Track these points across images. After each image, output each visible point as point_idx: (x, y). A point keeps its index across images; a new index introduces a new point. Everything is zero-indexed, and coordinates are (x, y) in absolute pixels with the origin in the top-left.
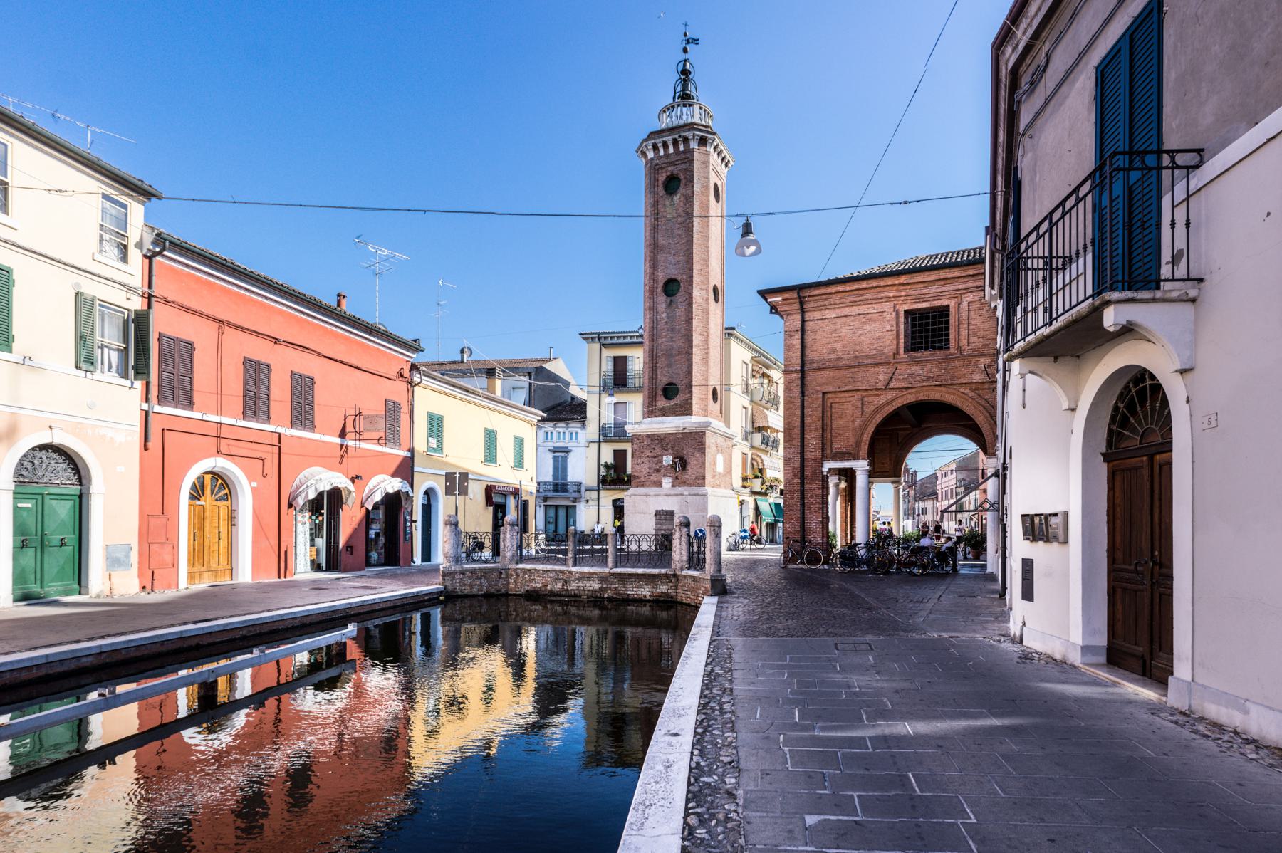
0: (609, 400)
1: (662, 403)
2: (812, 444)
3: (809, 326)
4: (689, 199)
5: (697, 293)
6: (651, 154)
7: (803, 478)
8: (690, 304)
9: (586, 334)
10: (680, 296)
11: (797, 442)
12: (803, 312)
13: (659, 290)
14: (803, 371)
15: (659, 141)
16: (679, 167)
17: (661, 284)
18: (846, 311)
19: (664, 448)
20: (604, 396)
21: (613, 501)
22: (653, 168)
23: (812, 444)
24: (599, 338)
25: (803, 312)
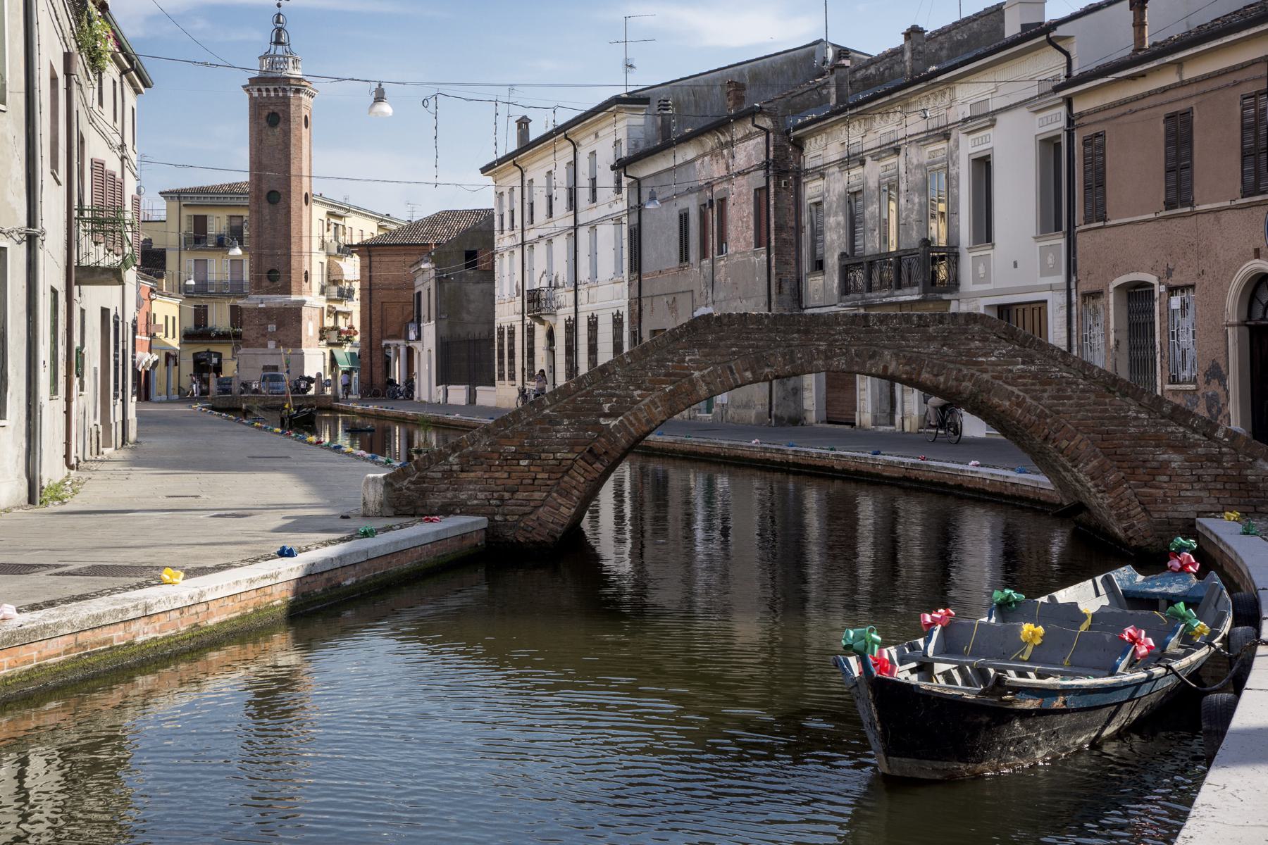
0: (188, 260)
1: (266, 283)
2: (376, 330)
3: (374, 264)
4: (287, 133)
5: (294, 205)
6: (256, 94)
7: (371, 349)
8: (289, 212)
9: (166, 193)
10: (281, 204)
11: (368, 329)
12: (370, 256)
13: (264, 198)
14: (370, 290)
15: (263, 88)
16: (279, 108)
17: (265, 194)
18: (394, 258)
19: (269, 319)
20: (184, 255)
21: (195, 355)
22: (256, 107)
23: (376, 330)
24: (179, 198)
25: (370, 256)
